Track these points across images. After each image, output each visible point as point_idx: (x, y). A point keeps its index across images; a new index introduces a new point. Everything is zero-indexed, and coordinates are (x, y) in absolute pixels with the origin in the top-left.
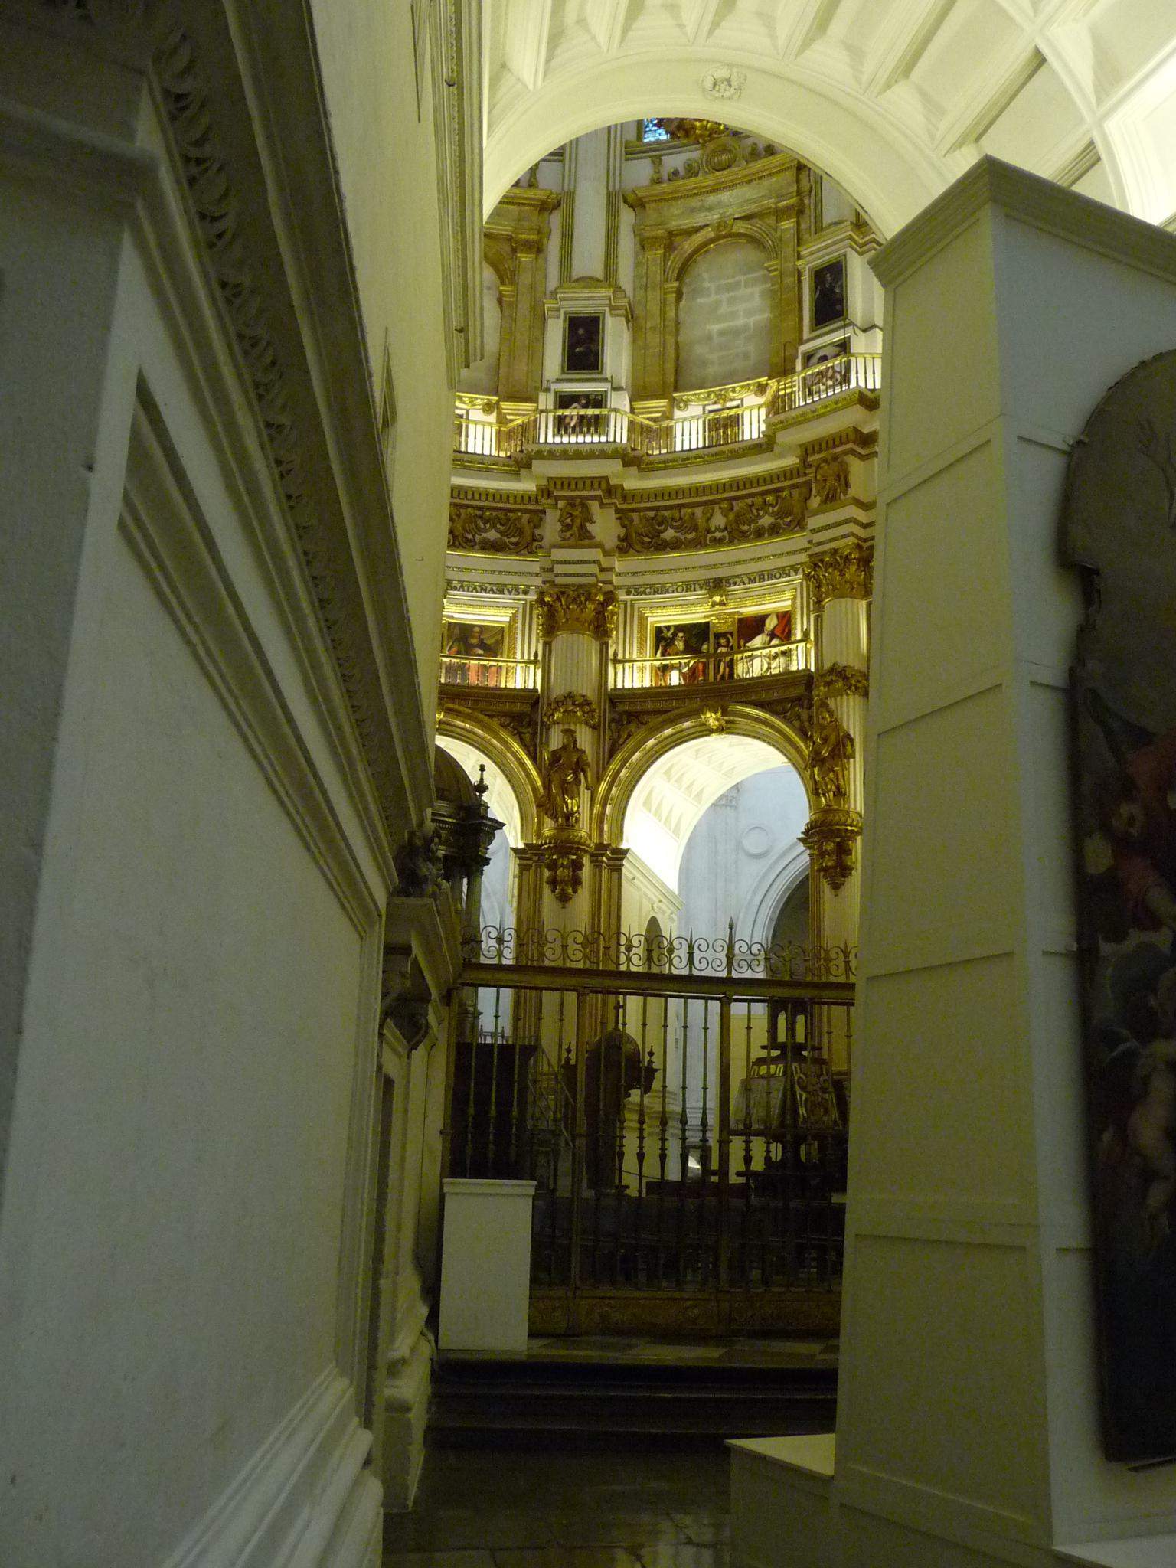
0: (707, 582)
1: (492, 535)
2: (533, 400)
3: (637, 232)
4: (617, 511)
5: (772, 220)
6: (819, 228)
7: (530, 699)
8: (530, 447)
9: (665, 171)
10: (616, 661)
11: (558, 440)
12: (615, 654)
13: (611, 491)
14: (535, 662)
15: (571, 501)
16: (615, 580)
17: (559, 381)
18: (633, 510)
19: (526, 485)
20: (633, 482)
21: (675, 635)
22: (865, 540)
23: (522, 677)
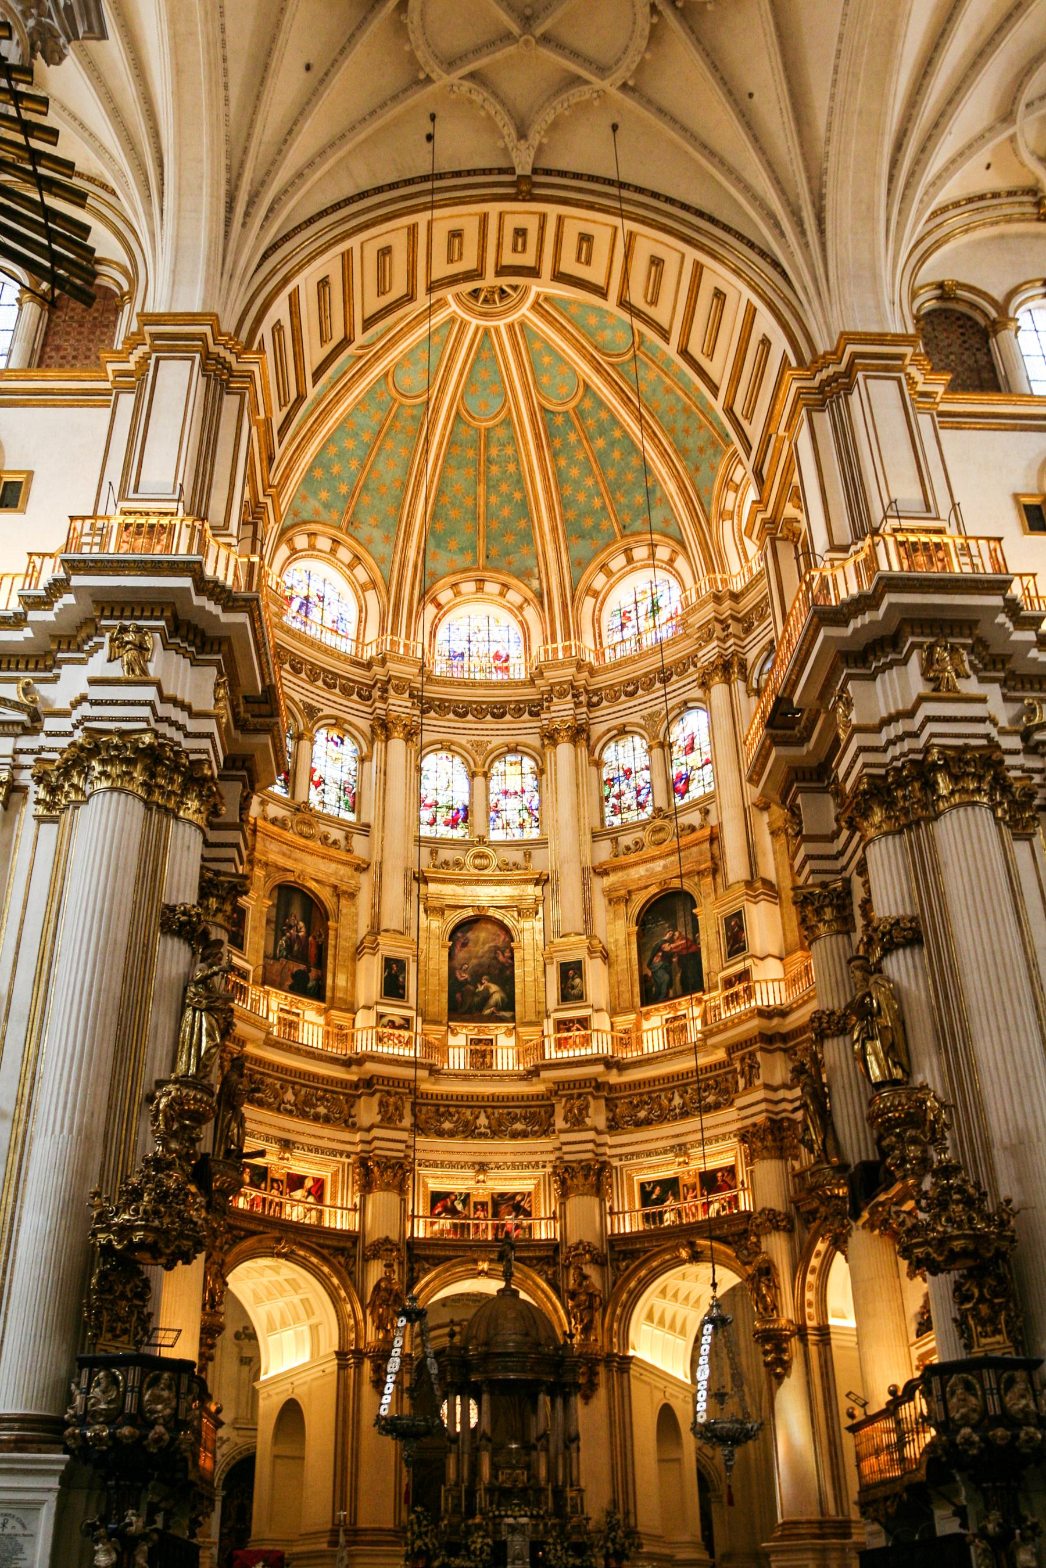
0: (673, 1147)
1: (519, 1126)
2: (539, 1024)
4: (607, 1099)
5: (696, 879)
6: (727, 887)
7: (554, 1246)
8: (540, 1062)
9: (621, 848)
10: (612, 1213)
11: (559, 1055)
12: (611, 1208)
13: (599, 1086)
14: (554, 1218)
15: (570, 1097)
16: (608, 1151)
17: (556, 1010)
18: (617, 1098)
19: (537, 1088)
20: (614, 1078)
21: (654, 1188)
22: (777, 1113)
23: (543, 1232)
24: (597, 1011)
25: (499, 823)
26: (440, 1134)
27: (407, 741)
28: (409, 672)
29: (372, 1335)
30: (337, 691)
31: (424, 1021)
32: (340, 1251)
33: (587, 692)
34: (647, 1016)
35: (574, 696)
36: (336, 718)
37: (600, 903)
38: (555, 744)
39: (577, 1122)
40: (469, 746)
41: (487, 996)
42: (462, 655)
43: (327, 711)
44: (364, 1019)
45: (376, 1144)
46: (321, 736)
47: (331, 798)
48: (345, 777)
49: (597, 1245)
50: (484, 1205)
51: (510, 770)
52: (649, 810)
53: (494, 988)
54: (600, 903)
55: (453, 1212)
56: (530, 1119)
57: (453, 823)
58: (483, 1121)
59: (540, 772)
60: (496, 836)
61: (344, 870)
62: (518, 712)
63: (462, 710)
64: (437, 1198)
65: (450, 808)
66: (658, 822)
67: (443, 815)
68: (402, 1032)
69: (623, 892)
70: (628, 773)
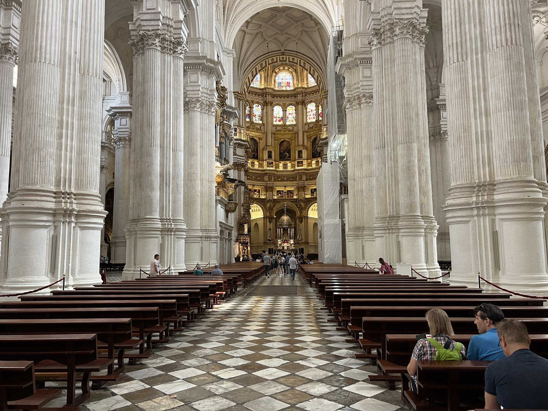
1: (291, 179)
3: (307, 136)
7: (296, 199)
9: (310, 127)
10: (306, 194)
13: (304, 173)
14: (297, 195)
15: (299, 175)
23: (295, 197)
24: (304, 159)
25: (288, 120)
26: (278, 181)
27: (270, 106)
28: (270, 91)
29: (268, 214)
30: (257, 96)
31: (275, 161)
32: (263, 201)
33: (304, 92)
34: (313, 160)
35: (302, 94)
36: (257, 102)
37: (305, 138)
38: (298, 105)
39: (300, 180)
40: (282, 104)
41: (286, 155)
42: (281, 83)
43: (255, 101)
44: (265, 163)
45: (268, 184)
46: (254, 106)
47: (257, 119)
48: (260, 114)
49: (303, 199)
50: (286, 192)
51: (290, 109)
52: (315, 119)
53: (287, 154)
54: (305, 138)
55: (281, 194)
56: (293, 178)
57: (280, 121)
58: (285, 178)
59: (296, 110)
60: (288, 123)
61: (260, 134)
62: (292, 96)
63: (281, 96)
64: (278, 191)
65: (279, 118)
66: (316, 123)
67: (278, 119)
68: (272, 165)
69: (310, 137)
70: (312, 110)
